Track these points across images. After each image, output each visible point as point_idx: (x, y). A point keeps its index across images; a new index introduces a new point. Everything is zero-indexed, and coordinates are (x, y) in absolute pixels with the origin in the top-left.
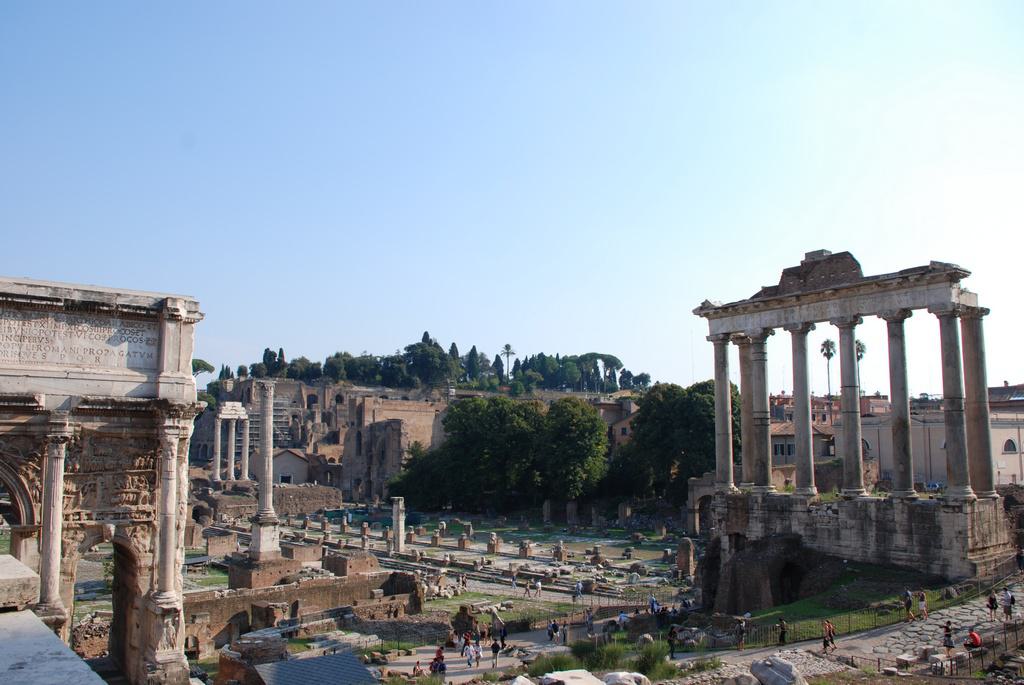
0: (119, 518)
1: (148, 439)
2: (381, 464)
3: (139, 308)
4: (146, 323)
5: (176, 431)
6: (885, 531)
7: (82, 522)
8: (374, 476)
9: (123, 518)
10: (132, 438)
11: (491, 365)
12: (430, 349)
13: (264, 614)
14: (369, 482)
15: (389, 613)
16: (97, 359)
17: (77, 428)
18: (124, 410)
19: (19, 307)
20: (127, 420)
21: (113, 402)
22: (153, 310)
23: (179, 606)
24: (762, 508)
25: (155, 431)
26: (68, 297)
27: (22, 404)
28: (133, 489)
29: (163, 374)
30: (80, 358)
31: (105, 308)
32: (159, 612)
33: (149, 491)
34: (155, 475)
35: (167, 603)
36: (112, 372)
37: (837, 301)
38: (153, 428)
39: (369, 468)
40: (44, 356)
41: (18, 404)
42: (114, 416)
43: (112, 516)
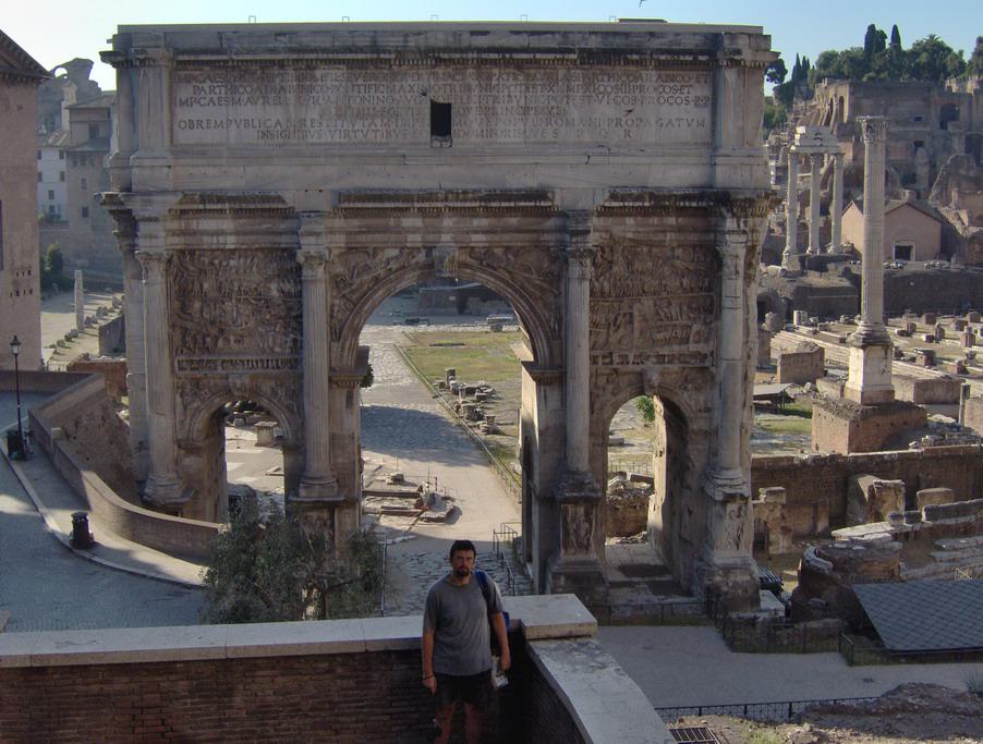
0: (664, 362)
1: (701, 246)
5: (743, 238)
7: (615, 366)
9: (669, 362)
10: (679, 246)
16: (628, 133)
19: (520, 66)
20: (672, 221)
21: (652, 196)
22: (702, 53)
25: (712, 236)
27: (532, 204)
28: (679, 322)
29: (722, 151)
30: (603, 132)
31: (635, 57)
32: (719, 497)
33: (705, 323)
34: (712, 300)
35: (731, 486)
40: (556, 133)
41: (528, 204)
42: (654, 214)
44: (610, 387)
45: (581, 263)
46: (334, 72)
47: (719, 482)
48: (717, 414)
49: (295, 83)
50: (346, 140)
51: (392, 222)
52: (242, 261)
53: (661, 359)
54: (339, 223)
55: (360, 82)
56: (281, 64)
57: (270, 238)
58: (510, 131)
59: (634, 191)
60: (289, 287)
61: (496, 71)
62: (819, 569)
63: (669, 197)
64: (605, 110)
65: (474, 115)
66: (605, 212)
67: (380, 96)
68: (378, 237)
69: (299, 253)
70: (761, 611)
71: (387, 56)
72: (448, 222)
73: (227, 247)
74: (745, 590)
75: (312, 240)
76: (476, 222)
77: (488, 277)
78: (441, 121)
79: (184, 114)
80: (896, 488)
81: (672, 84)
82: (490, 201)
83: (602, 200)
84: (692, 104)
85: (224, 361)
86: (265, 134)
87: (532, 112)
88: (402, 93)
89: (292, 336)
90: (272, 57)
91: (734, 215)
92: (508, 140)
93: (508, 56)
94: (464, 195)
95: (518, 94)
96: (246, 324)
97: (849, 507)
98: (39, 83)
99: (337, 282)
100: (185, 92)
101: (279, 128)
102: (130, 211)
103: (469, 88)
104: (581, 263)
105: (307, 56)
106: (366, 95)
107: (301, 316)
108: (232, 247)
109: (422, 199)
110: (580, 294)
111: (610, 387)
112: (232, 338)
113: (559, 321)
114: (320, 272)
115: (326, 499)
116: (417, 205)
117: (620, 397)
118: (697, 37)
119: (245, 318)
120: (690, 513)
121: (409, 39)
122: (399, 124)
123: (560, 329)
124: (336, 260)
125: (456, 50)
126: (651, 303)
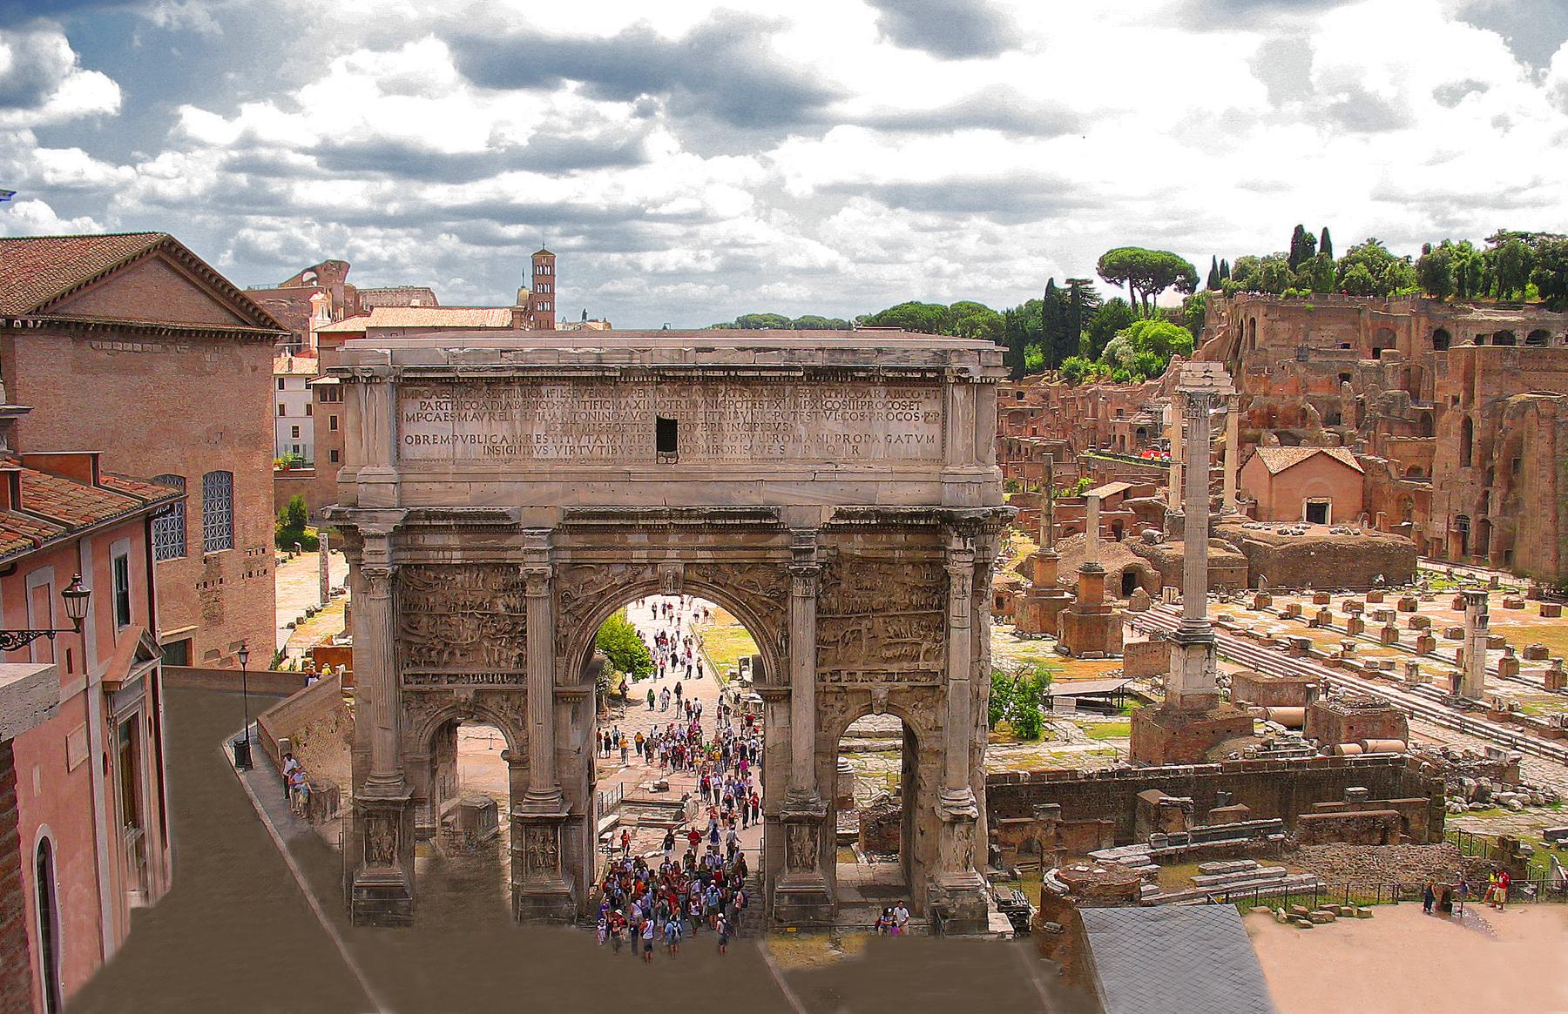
1: (931, 564)
2: (1511, 485)
3: (912, 370)
4: (923, 390)
8: (1494, 510)
9: (898, 681)
10: (909, 563)
14: (1485, 523)
15: (1371, 830)
16: (855, 449)
17: (831, 552)
18: (896, 525)
19: (746, 382)
20: (901, 538)
21: (878, 514)
23: (972, 811)
26: (809, 363)
27: (758, 521)
31: (862, 374)
35: (958, 808)
36: (876, 468)
38: (937, 549)
39: (1486, 494)
40: (783, 451)
41: (752, 521)
43: (884, 677)
44: (839, 705)
45: (805, 581)
46: (559, 388)
47: (946, 802)
48: (947, 734)
49: (521, 399)
50: (571, 457)
51: (617, 538)
52: (467, 575)
53: (890, 676)
54: (564, 540)
55: (586, 398)
56: (508, 381)
57: (495, 554)
58: (738, 450)
59: (860, 508)
60: (513, 602)
61: (722, 388)
62: (1054, 892)
63: (896, 515)
64: (832, 426)
65: (699, 431)
66: (831, 530)
67: (604, 410)
68: (603, 553)
69: (522, 569)
70: (990, 933)
71: (612, 374)
72: (673, 539)
73: (453, 562)
74: (973, 913)
75: (536, 558)
76: (702, 539)
77: (714, 594)
78: (667, 435)
79: (411, 429)
80: (1184, 805)
81: (901, 400)
82: (714, 519)
83: (826, 517)
84: (922, 420)
85: (449, 675)
86: (493, 449)
87: (759, 429)
88: (627, 408)
89: (518, 651)
90: (498, 374)
91: (960, 534)
92: (734, 456)
93: (733, 373)
94: (689, 513)
95: (744, 410)
96: (472, 638)
98: (275, 341)
99: (562, 599)
100: (411, 407)
101: (504, 442)
102: (356, 527)
103: (695, 405)
104: (805, 581)
105: (532, 374)
106: (592, 412)
107: (524, 631)
108: (458, 562)
109: (646, 516)
110: (802, 614)
111: (839, 705)
112: (458, 653)
113: (786, 637)
114: (544, 590)
115: (548, 815)
116: (640, 522)
117: (849, 714)
118: (926, 354)
119: (470, 633)
120: (922, 833)
121: (636, 356)
122: (625, 441)
123: (787, 648)
124: (562, 575)
125: (680, 369)
126: (881, 620)
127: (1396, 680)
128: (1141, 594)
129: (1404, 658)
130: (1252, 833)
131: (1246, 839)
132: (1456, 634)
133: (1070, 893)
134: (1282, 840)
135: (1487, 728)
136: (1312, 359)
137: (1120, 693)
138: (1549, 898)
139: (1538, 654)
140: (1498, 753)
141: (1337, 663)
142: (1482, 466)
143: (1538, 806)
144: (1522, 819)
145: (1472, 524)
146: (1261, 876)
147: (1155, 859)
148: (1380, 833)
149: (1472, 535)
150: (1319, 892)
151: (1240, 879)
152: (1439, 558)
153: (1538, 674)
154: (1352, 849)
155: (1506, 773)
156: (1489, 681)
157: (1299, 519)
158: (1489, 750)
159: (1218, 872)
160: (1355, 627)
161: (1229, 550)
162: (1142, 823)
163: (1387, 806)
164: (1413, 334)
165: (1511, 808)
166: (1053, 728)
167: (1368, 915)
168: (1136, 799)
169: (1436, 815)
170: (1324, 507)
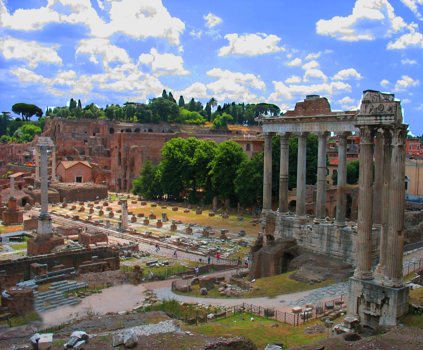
2: (132, 170)
6: (330, 241)
8: (128, 177)
11: (204, 109)
12: (166, 101)
13: (35, 270)
14: (126, 181)
15: (100, 268)
24: (281, 224)
37: (318, 123)
39: (126, 173)
62: (6, 298)
97: (31, 274)
127: (104, 225)
128: (28, 205)
129: (105, 219)
130: (66, 272)
131: (64, 275)
132: (119, 211)
133: (11, 297)
134: (75, 274)
135: (129, 236)
136: (77, 136)
137: (23, 235)
138: (149, 281)
139: (141, 215)
140: (133, 243)
141: (87, 222)
142: (124, 165)
143: (144, 256)
144: (140, 260)
145: (122, 181)
146: (69, 285)
147: (37, 283)
148: (102, 268)
149: (122, 184)
150: (86, 287)
151: (63, 286)
152: (113, 191)
153: (142, 221)
154: (95, 274)
155: (135, 248)
156: (129, 224)
157: (74, 181)
158: (130, 243)
159: (56, 285)
160: (92, 211)
161: (54, 191)
162: (32, 273)
163: (104, 261)
164: (104, 129)
165: (137, 258)
166: (2, 247)
167: (101, 292)
168: (30, 266)
169: (117, 261)
170: (81, 178)
